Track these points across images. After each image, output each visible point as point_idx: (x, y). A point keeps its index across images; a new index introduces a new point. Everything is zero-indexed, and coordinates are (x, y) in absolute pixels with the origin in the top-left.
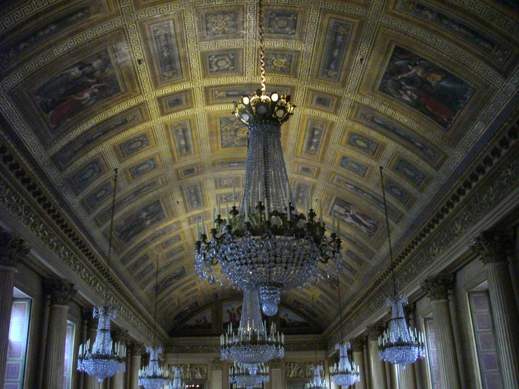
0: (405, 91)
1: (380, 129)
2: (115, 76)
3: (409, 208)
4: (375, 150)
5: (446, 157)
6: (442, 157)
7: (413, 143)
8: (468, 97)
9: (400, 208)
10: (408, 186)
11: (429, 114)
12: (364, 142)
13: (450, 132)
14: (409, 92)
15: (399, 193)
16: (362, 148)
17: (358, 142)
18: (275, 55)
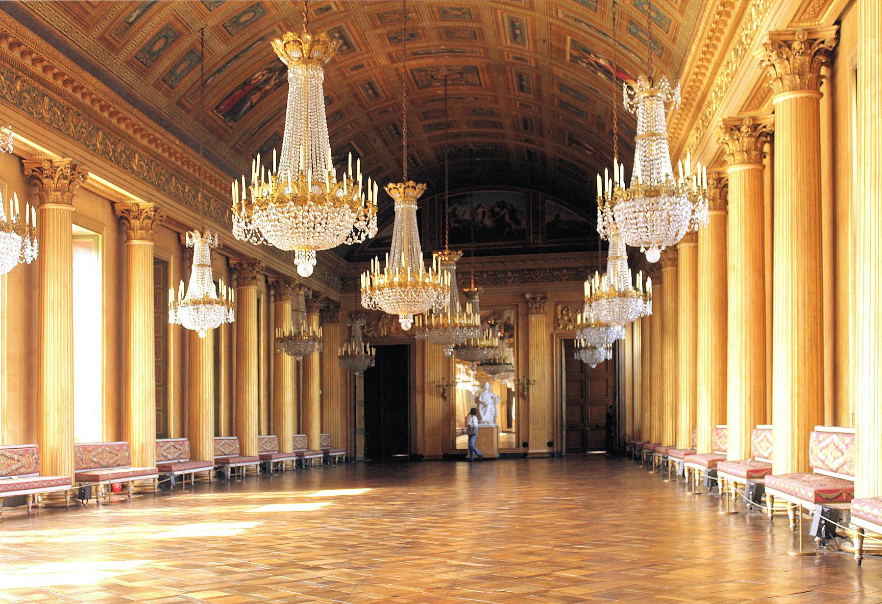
0: (263, 75)
1: (249, 44)
2: (571, 48)
3: (129, 63)
4: (227, 30)
5: (188, 111)
6: (190, 107)
7: (213, 75)
8: (230, 124)
9: (131, 48)
10: (165, 64)
11: (232, 93)
12: (246, 21)
13: (209, 112)
14: (260, 78)
15: (156, 48)
16: (241, 16)
17: (251, 15)
18: (399, 20)
